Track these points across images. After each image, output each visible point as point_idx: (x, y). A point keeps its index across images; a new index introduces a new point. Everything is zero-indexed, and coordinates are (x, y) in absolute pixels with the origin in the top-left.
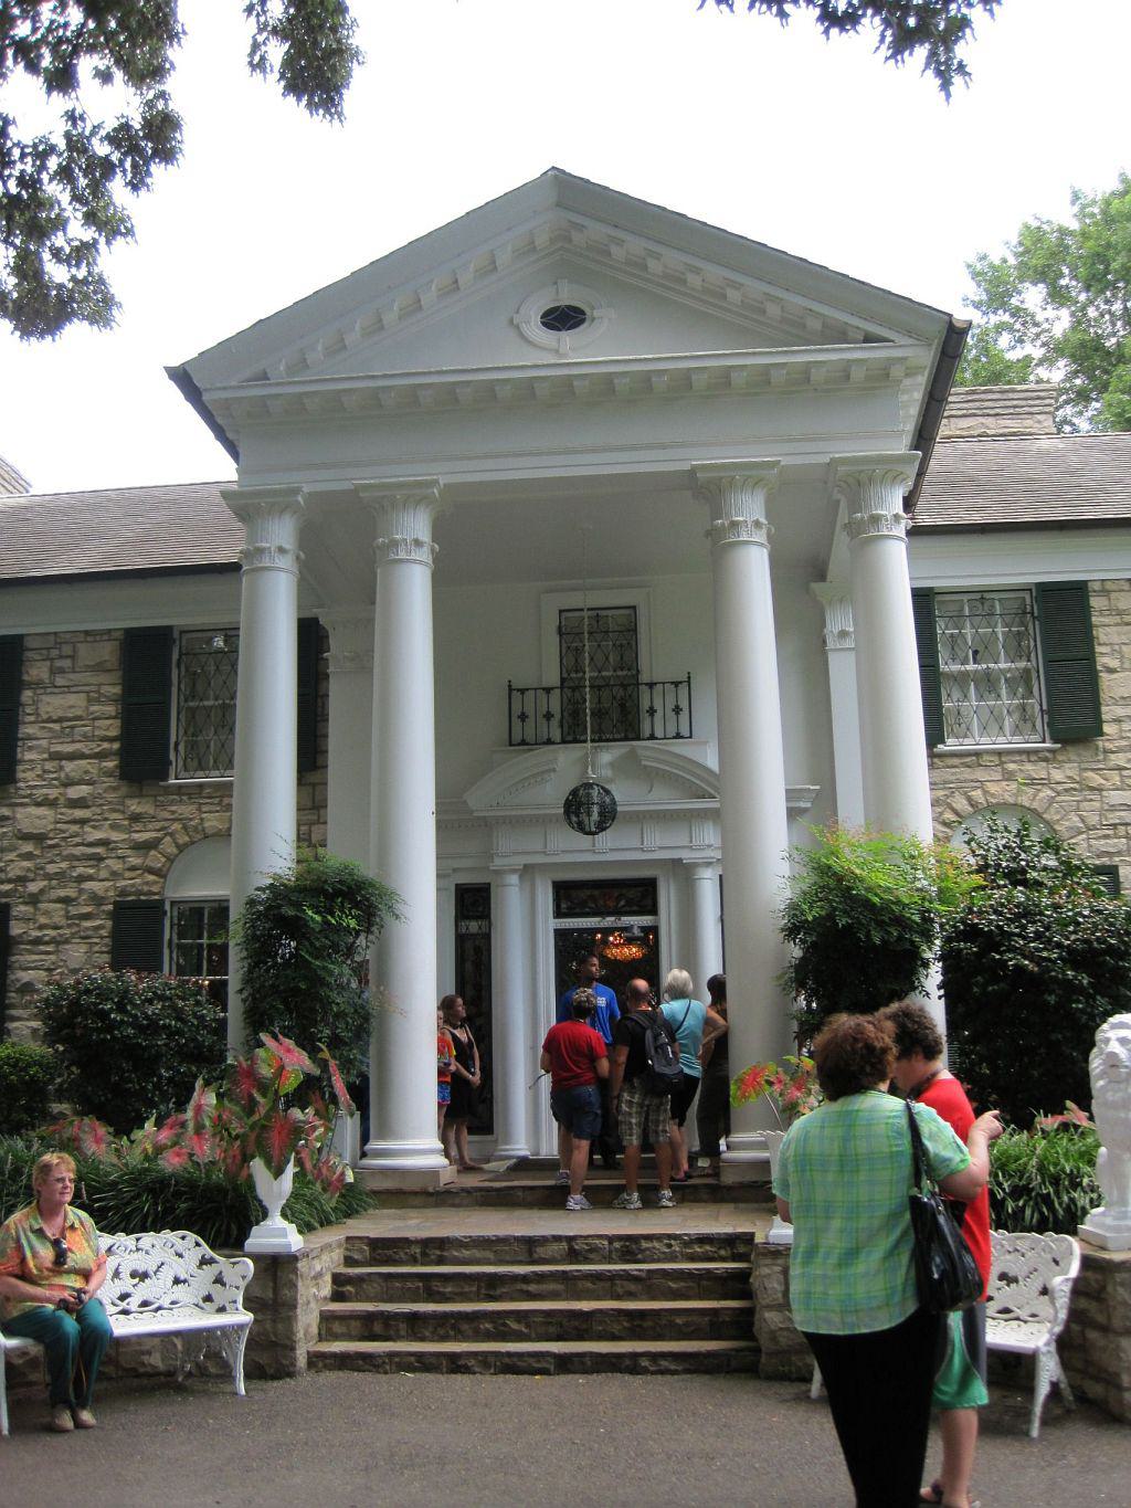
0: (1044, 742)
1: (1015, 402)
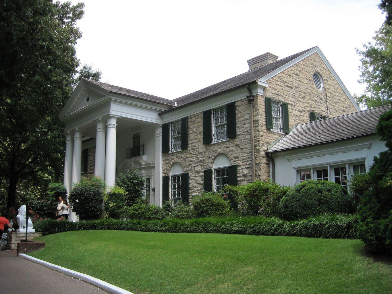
1: (261, 59)
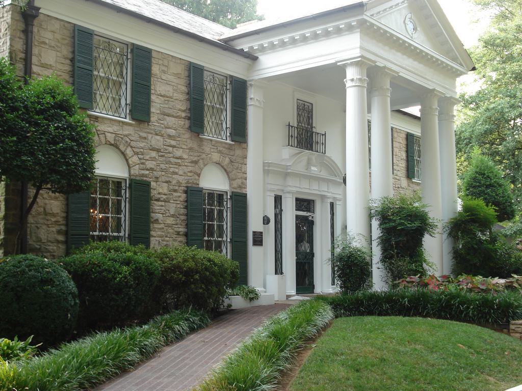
0: (126, 118)
